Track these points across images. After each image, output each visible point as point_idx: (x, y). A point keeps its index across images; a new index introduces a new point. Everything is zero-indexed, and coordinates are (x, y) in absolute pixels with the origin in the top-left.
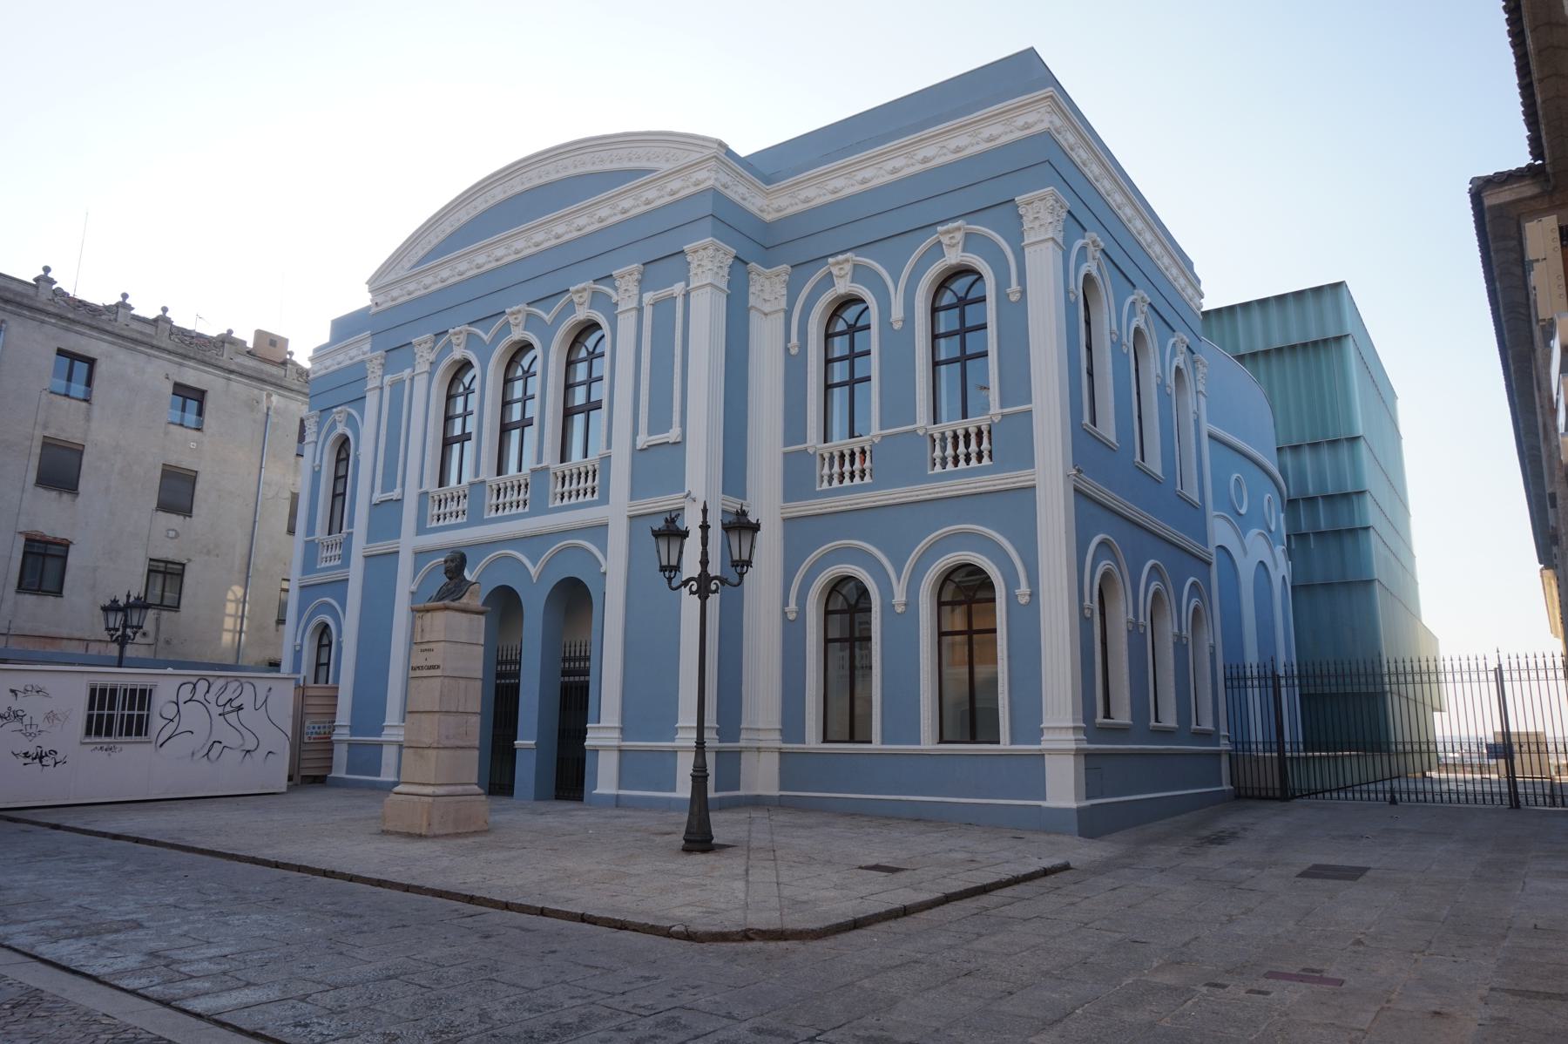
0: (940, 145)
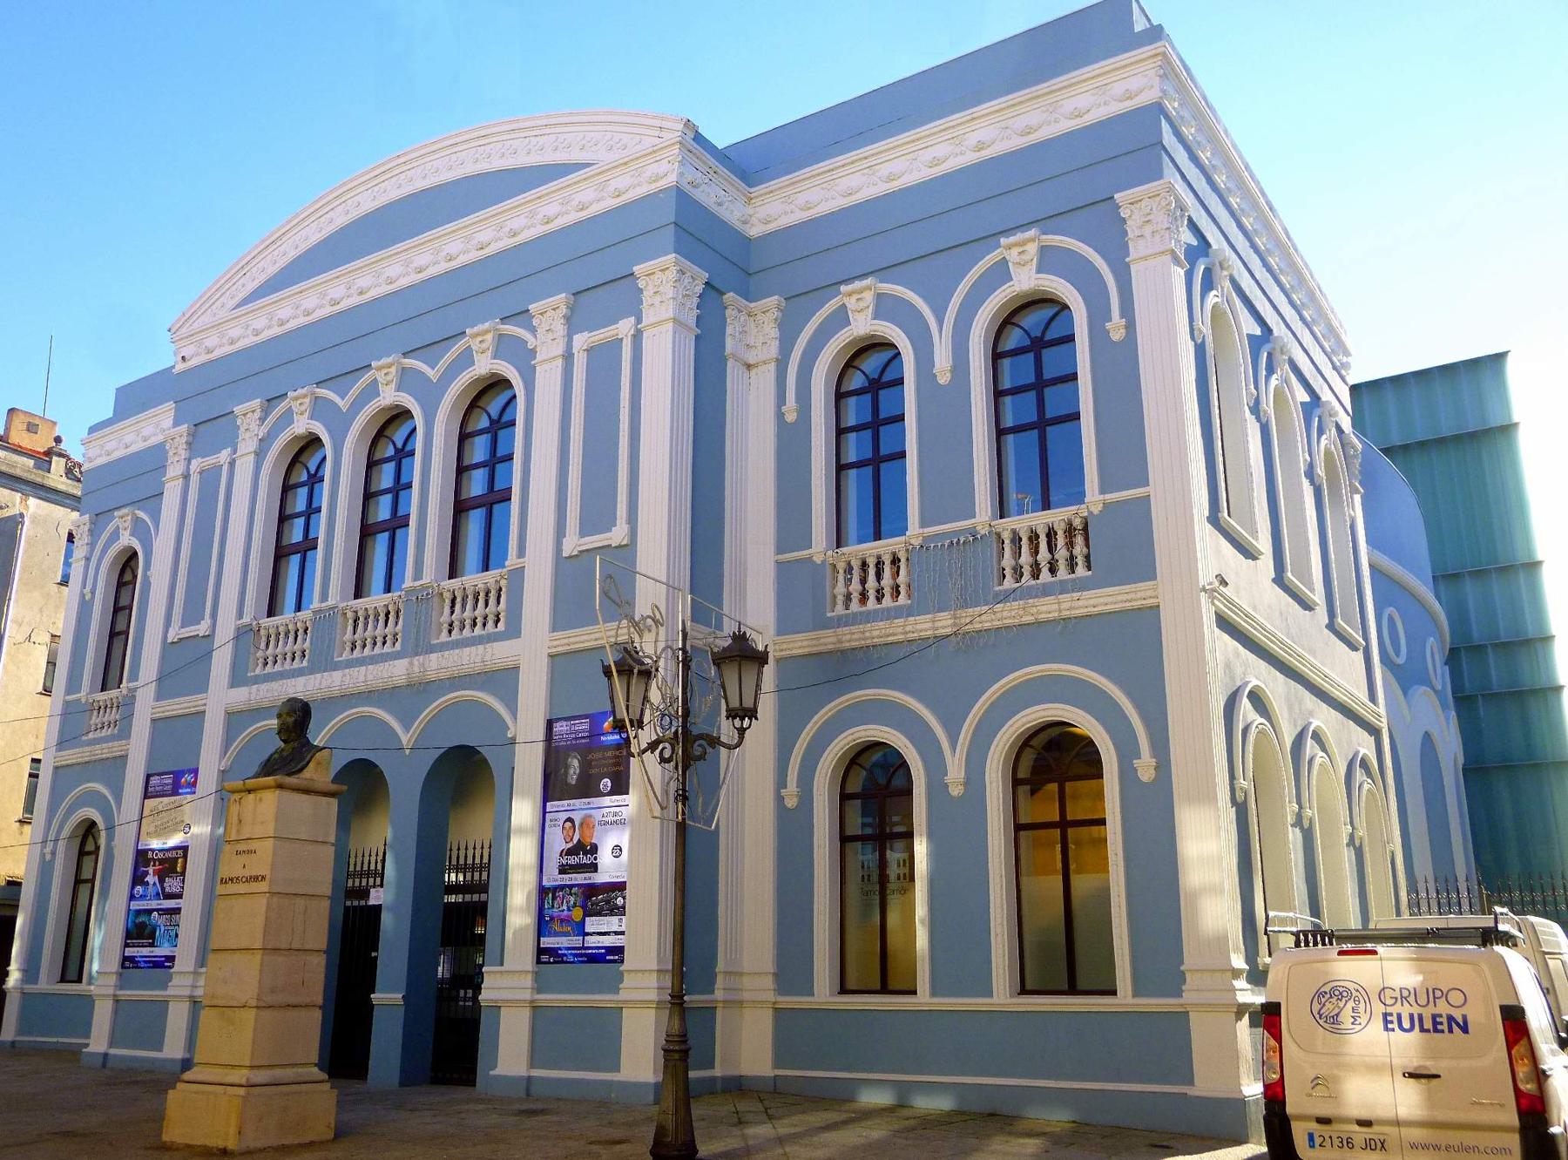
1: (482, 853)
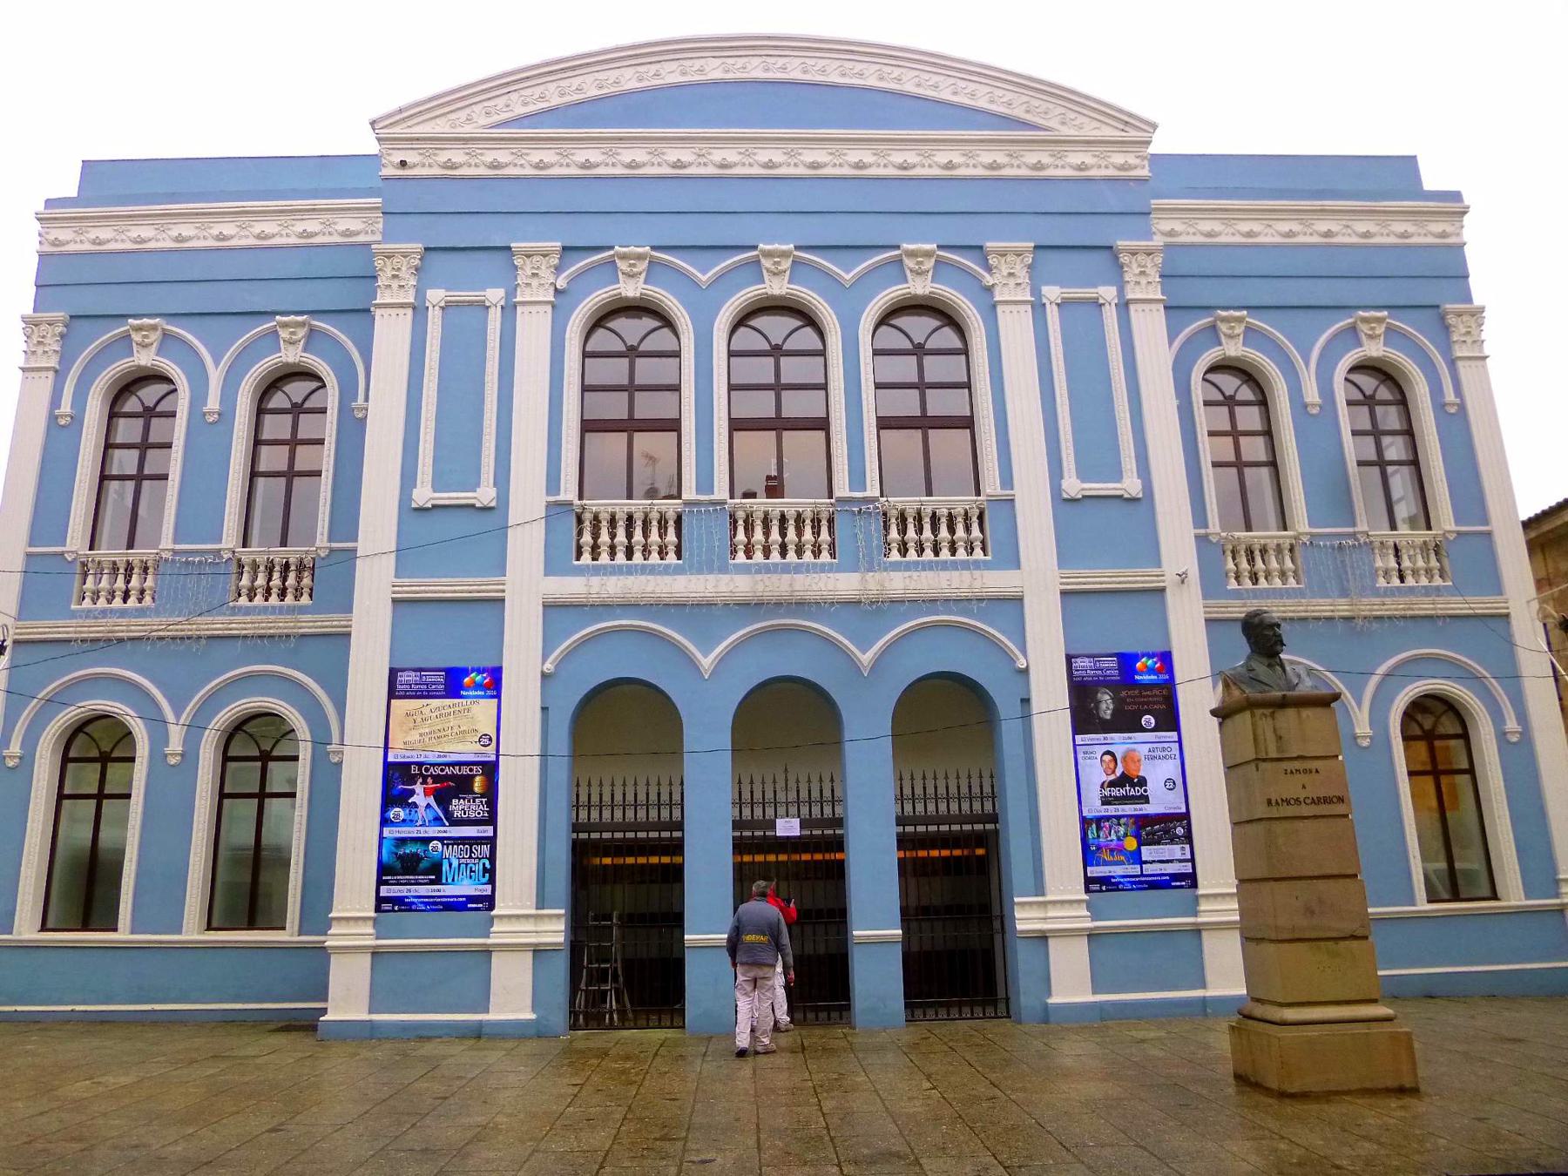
0: (1344, 222)
1: (970, 783)
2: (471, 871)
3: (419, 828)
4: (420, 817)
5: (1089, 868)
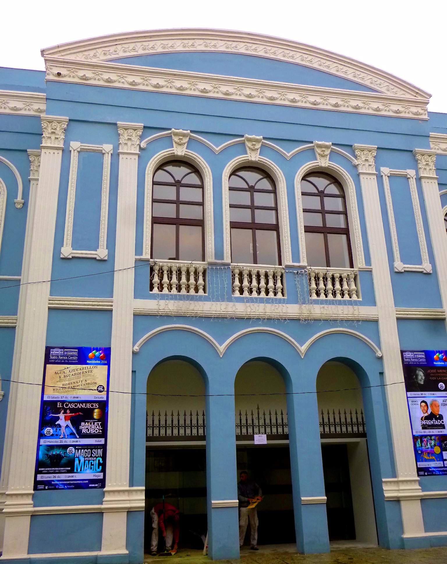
2: (92, 465)
3: (62, 440)
4: (62, 433)
5: (418, 463)
